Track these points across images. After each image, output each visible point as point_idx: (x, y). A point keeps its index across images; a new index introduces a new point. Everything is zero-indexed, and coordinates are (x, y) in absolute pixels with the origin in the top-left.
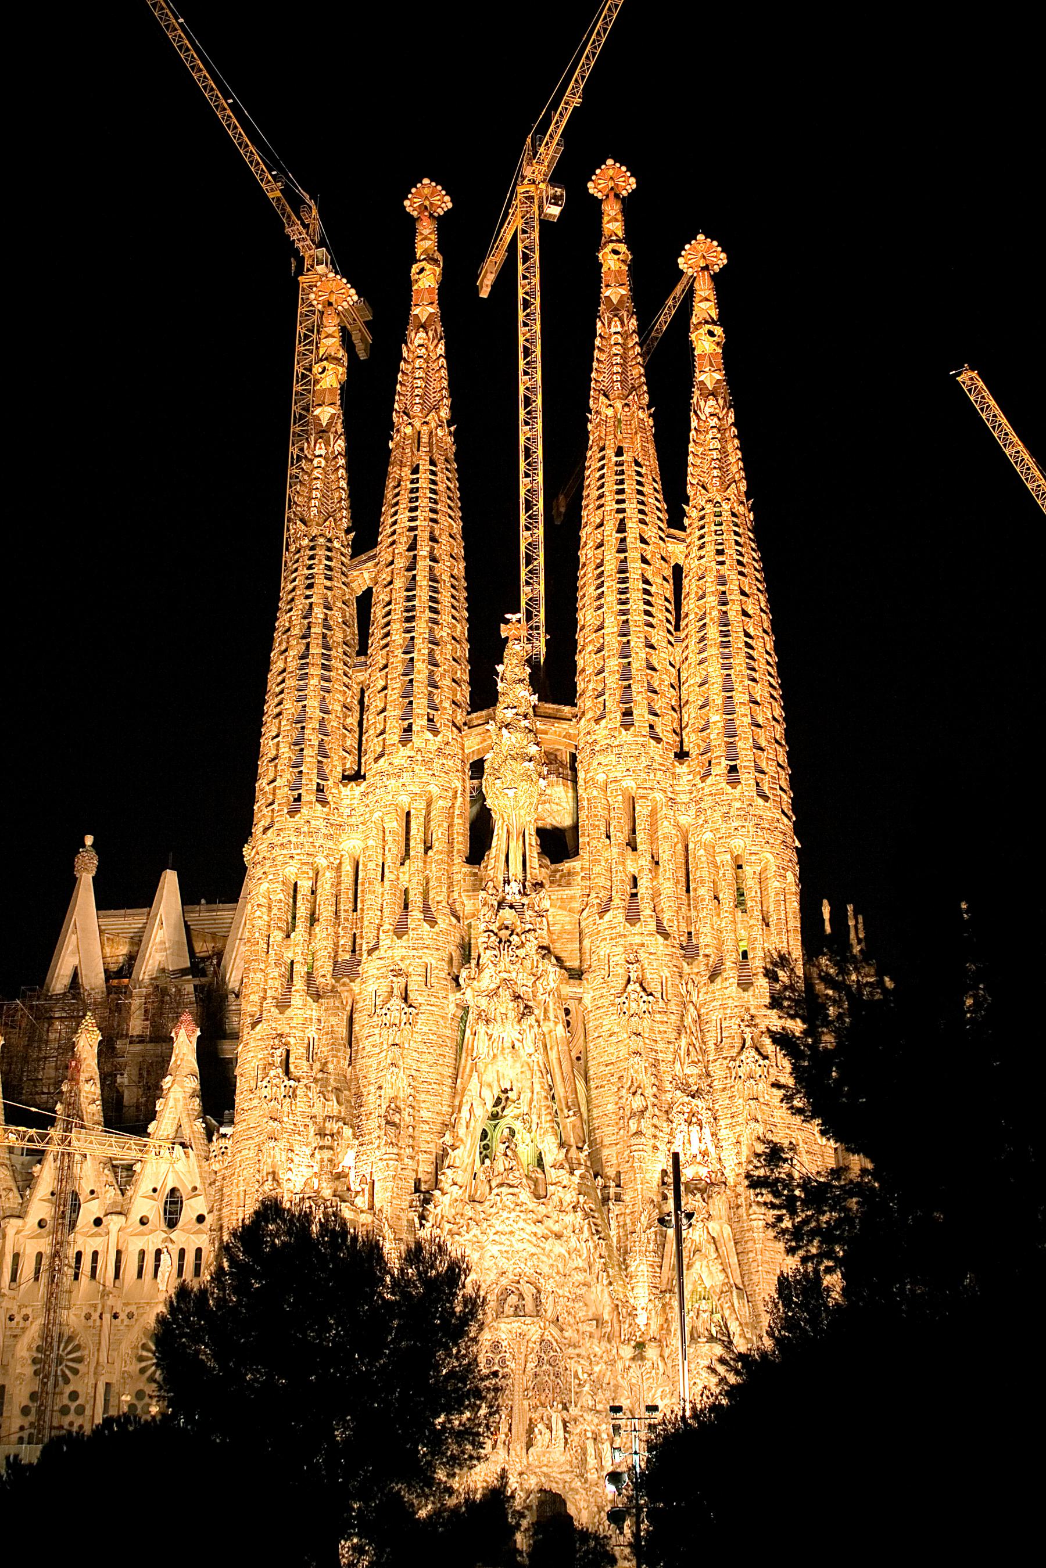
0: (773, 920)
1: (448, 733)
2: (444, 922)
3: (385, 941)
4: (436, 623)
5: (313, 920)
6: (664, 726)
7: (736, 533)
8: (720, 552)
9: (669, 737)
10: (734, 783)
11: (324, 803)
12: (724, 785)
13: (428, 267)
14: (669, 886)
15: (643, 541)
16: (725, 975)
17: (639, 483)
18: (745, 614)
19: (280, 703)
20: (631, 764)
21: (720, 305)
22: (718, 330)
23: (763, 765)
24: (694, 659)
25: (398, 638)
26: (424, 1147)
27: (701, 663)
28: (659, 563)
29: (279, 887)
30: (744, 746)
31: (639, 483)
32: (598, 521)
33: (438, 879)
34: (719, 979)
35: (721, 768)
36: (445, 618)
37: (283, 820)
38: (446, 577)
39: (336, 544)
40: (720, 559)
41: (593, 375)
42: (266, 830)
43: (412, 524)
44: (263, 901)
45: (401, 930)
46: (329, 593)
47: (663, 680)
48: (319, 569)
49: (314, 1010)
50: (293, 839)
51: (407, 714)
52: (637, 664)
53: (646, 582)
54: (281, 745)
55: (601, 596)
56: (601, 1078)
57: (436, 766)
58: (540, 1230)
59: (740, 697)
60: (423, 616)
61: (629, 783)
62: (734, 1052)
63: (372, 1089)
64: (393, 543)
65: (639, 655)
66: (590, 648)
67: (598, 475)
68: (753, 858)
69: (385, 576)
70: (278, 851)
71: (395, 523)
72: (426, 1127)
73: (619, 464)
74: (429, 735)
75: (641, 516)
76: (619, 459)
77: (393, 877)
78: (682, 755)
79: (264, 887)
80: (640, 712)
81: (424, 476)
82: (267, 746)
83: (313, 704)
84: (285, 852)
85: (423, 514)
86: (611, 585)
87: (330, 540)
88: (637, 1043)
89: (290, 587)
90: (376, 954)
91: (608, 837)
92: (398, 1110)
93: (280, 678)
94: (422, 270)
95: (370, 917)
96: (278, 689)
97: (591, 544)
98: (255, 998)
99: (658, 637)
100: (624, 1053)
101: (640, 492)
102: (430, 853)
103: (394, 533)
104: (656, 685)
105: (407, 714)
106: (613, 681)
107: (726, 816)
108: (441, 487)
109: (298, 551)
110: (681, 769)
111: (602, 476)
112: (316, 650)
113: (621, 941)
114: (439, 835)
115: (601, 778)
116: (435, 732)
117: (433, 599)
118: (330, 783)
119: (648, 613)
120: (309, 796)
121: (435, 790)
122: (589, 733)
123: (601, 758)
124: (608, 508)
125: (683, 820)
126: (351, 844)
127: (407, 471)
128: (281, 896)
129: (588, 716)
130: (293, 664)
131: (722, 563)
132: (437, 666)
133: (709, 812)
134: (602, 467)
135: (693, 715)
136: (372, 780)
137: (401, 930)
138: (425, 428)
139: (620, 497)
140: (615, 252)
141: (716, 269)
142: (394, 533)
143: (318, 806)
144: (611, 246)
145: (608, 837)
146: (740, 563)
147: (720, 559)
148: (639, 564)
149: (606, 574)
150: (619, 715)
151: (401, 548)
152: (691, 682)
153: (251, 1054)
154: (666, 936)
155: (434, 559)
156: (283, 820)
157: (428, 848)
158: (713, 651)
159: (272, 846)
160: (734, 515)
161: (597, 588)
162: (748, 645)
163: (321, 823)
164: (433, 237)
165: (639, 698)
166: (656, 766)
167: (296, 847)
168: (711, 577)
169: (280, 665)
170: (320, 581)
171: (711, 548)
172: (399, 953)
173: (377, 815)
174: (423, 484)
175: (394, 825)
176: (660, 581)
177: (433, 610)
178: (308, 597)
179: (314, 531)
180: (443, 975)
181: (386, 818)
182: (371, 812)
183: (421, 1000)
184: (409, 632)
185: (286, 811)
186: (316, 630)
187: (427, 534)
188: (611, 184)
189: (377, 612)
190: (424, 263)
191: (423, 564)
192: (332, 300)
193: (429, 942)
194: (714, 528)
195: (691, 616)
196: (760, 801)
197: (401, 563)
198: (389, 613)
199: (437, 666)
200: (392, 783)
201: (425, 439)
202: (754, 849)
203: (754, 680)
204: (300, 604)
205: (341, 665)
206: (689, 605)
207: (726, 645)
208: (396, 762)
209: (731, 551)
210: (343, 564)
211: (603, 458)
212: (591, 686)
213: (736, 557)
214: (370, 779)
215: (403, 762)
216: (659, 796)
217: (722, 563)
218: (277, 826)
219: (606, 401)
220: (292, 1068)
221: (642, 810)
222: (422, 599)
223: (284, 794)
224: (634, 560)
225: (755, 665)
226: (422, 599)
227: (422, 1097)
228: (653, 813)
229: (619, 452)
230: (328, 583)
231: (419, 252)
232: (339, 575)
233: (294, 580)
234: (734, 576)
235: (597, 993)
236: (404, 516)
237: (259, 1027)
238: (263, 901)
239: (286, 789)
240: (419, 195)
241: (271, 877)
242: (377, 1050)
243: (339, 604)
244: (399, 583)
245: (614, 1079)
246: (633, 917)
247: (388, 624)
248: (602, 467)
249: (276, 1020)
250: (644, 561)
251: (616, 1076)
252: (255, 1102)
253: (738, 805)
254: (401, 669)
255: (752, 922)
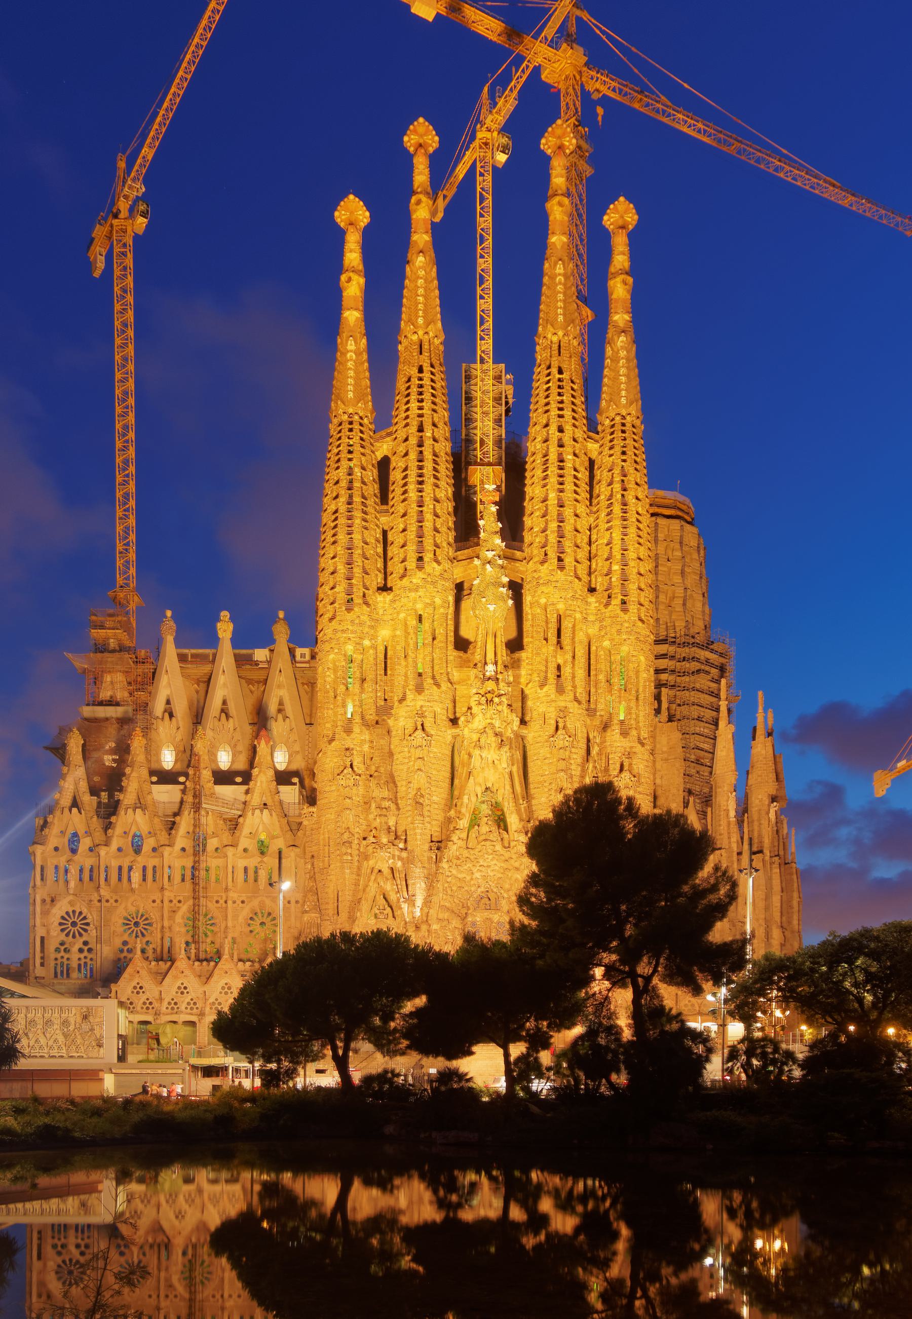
0: (641, 697)
1: (446, 565)
2: (445, 686)
3: (410, 696)
4: (437, 486)
5: (363, 680)
6: (582, 570)
7: (635, 440)
8: (624, 453)
9: (585, 578)
10: (625, 611)
11: (366, 603)
12: (619, 611)
13: (424, 198)
14: (581, 673)
15: (575, 440)
16: (613, 728)
17: (573, 396)
18: (637, 498)
19: (334, 535)
20: (563, 594)
21: (633, 258)
22: (630, 280)
23: (642, 600)
24: (603, 526)
25: (413, 495)
26: (435, 817)
27: (608, 530)
28: (583, 457)
29: (342, 658)
30: (632, 587)
31: (573, 396)
32: (545, 422)
33: (440, 659)
34: (609, 730)
35: (616, 601)
36: (442, 484)
37: (342, 613)
38: (442, 454)
39: (366, 421)
40: (624, 457)
41: (542, 307)
42: (331, 620)
43: (420, 412)
44: (331, 666)
45: (419, 689)
46: (363, 458)
47: (582, 539)
48: (356, 440)
49: (366, 736)
50: (350, 628)
51: (420, 550)
52: (568, 528)
53: (575, 470)
54: (338, 564)
55: (545, 478)
56: (540, 782)
57: (440, 587)
58: (504, 865)
59: (631, 555)
60: (429, 481)
61: (561, 606)
62: (616, 772)
63: (404, 783)
64: (407, 425)
65: (570, 520)
66: (537, 514)
67: (546, 387)
68: (634, 659)
69: (402, 449)
70: (339, 635)
71: (408, 410)
72: (436, 806)
73: (560, 380)
74: (435, 565)
75: (573, 421)
76: (561, 376)
77: (413, 656)
78: (592, 590)
79: (332, 656)
80: (569, 560)
81: (426, 375)
82: (326, 563)
83: (357, 536)
84: (345, 635)
85: (427, 405)
86: (553, 470)
87: (361, 418)
88: (562, 765)
89: (336, 451)
90: (405, 702)
91: (546, 639)
92: (422, 796)
93: (334, 517)
94: (419, 202)
95: (399, 680)
96: (333, 525)
97: (539, 439)
98: (328, 725)
99: (582, 509)
100: (553, 769)
101: (573, 403)
102: (435, 642)
103: (407, 417)
104: (578, 542)
105: (420, 550)
106: (553, 538)
107: (619, 632)
108: (438, 385)
109: (340, 424)
110: (592, 599)
111: (548, 389)
112: (357, 499)
113: (553, 704)
114: (440, 631)
115: (543, 601)
116: (439, 563)
117: (435, 469)
118: (370, 592)
119: (576, 492)
120: (358, 600)
121: (438, 601)
122: (535, 571)
123: (544, 589)
124: (553, 413)
125: (590, 631)
126: (384, 633)
127: (414, 372)
128: (344, 663)
129: (536, 559)
130: (343, 508)
131: (624, 461)
132: (438, 516)
133: (608, 629)
134: (548, 382)
135: (600, 564)
136: (398, 592)
137: (419, 689)
138: (426, 337)
139: (561, 406)
140: (560, 204)
141: (631, 227)
142: (407, 417)
143: (365, 607)
144: (557, 199)
145: (546, 639)
146: (636, 462)
147: (624, 457)
148: (570, 457)
149: (550, 462)
150: (556, 560)
151: (413, 429)
152: (600, 542)
153: (328, 759)
154: (579, 703)
155: (435, 440)
156: (342, 613)
157: (434, 639)
158: (617, 522)
159: (335, 631)
160: (633, 426)
161: (544, 471)
162: (638, 521)
163: (364, 618)
164: (427, 171)
165: (568, 550)
166: (577, 596)
167: (352, 632)
168: (617, 471)
169: (333, 507)
170: (357, 448)
171: (618, 450)
172: (420, 703)
173: (402, 615)
174: (426, 382)
175: (413, 622)
176: (583, 469)
177: (436, 477)
178: (350, 460)
179: (351, 411)
180: (444, 718)
181: (409, 618)
182: (398, 613)
183: (432, 732)
184: (420, 491)
185: (344, 608)
186: (357, 484)
187: (430, 420)
188: (558, 142)
189: (396, 476)
190: (421, 196)
191: (428, 443)
192: (353, 219)
193: (436, 698)
194: (620, 434)
195: (602, 497)
196: (640, 624)
197: (413, 441)
198: (405, 477)
199: (438, 516)
200: (412, 595)
201: (426, 346)
202: (635, 653)
203: (639, 544)
204: (344, 464)
205: (373, 511)
206: (602, 490)
207: (625, 519)
208: (415, 581)
209: (630, 453)
210: (371, 437)
211: (549, 375)
212: (537, 540)
213: (634, 457)
214: (396, 591)
215: (419, 581)
216: (578, 616)
217: (624, 461)
218: (338, 618)
219: (552, 329)
220: (355, 769)
221: (567, 624)
222: (428, 470)
223: (342, 597)
224: (569, 454)
225: (641, 533)
226: (428, 470)
227: (433, 789)
228: (574, 626)
229: (560, 372)
230: (362, 450)
231: (416, 184)
232: (369, 445)
233: (339, 446)
234: (632, 471)
235: (537, 734)
236: (414, 405)
237: (333, 744)
238: (331, 666)
239: (343, 594)
240: (415, 132)
241: (336, 651)
242: (406, 761)
243: (370, 467)
244: (413, 456)
245: (546, 784)
246: (560, 690)
247: (405, 484)
248: (548, 382)
249: (344, 739)
250: (575, 455)
251: (548, 782)
252: (333, 788)
253: (626, 625)
254: (415, 518)
255: (630, 697)
